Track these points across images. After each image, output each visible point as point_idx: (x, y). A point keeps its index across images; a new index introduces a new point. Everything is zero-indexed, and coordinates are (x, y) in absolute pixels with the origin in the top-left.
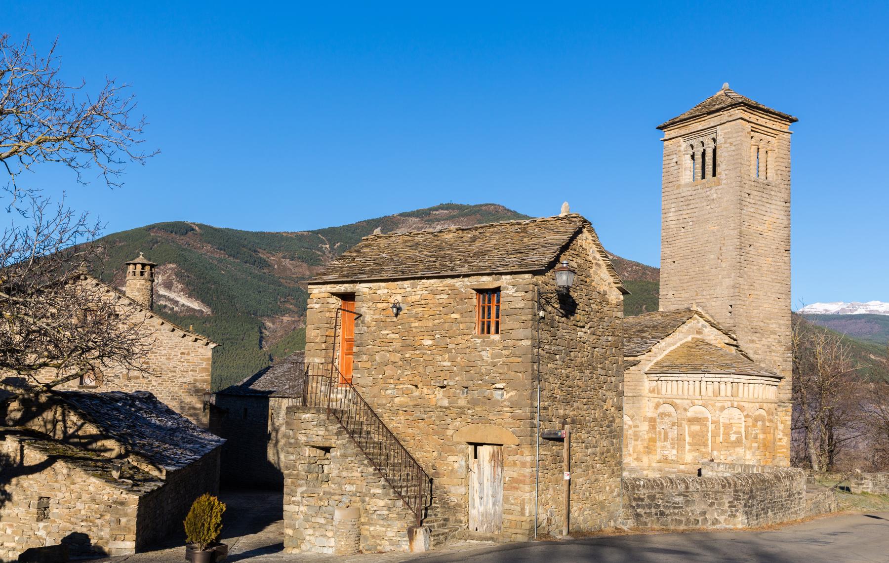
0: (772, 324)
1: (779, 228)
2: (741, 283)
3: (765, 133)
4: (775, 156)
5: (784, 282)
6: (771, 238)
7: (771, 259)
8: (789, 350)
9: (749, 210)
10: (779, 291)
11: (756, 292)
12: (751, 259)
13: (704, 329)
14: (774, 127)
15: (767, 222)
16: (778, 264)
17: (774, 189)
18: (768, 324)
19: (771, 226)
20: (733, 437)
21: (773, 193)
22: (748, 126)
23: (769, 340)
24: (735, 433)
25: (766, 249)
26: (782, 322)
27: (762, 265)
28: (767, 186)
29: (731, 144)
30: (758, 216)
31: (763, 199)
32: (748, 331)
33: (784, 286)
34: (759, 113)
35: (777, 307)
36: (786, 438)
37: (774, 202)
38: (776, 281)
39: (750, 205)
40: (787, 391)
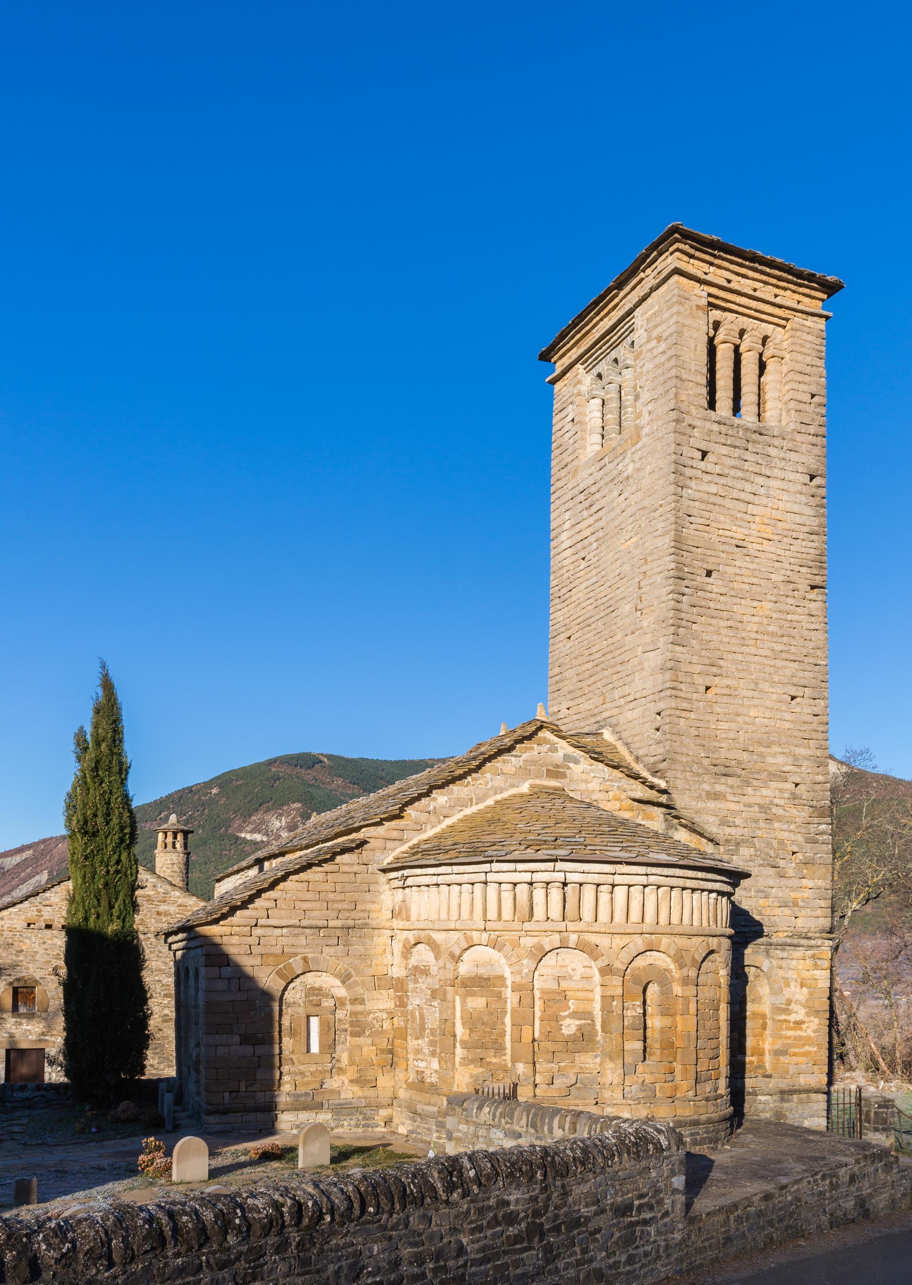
0: (774, 755)
1: (795, 535)
2: (681, 657)
3: (752, 313)
4: (785, 369)
5: (806, 660)
6: (772, 556)
7: (770, 605)
8: (822, 815)
9: (704, 487)
10: (795, 680)
11: (726, 681)
12: (712, 604)
13: (571, 765)
14: (778, 300)
15: (757, 519)
16: (789, 617)
17: (776, 443)
18: (761, 755)
19: (769, 529)
20: (569, 1027)
21: (773, 452)
22: (700, 293)
23: (765, 792)
24: (575, 1015)
25: (755, 581)
26: (803, 751)
27: (745, 619)
28: (756, 436)
29: (659, 339)
30: (728, 503)
31: (747, 466)
32: (701, 771)
33: (808, 668)
34: (732, 262)
35: (788, 716)
36: (817, 1021)
37: (776, 472)
38: (784, 655)
39: (707, 478)
40: (819, 912)
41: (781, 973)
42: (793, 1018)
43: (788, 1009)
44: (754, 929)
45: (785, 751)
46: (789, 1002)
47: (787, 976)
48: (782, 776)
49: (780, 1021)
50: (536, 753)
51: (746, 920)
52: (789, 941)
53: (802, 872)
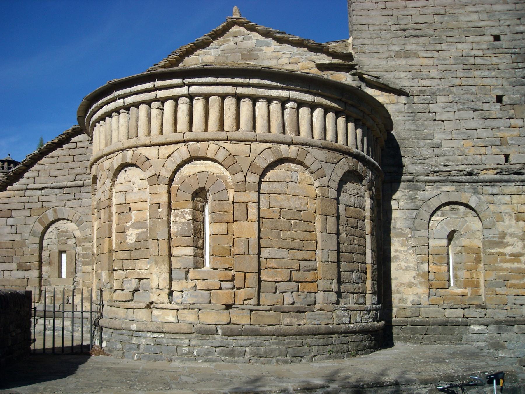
13: (264, 48)
23: (460, 46)
32: (388, 36)
41: (492, 207)
42: (508, 250)
43: (502, 242)
44: (457, 168)
45: (479, 9)
46: (503, 235)
47: (500, 211)
48: (480, 31)
49: (494, 254)
50: (232, 43)
51: (447, 160)
52: (497, 177)
53: (508, 112)
